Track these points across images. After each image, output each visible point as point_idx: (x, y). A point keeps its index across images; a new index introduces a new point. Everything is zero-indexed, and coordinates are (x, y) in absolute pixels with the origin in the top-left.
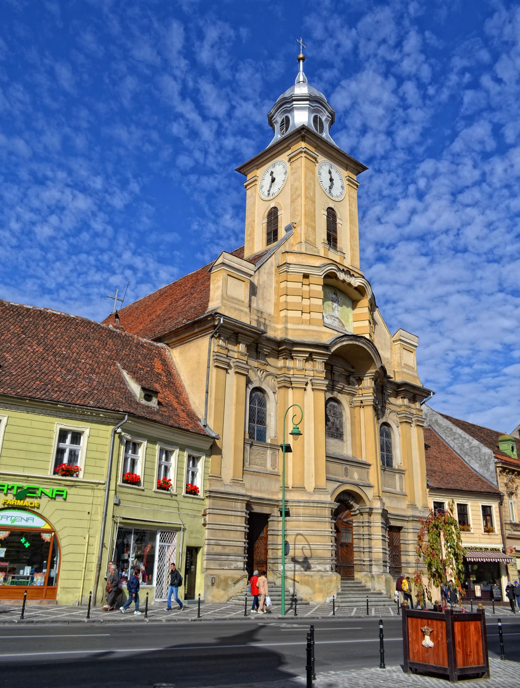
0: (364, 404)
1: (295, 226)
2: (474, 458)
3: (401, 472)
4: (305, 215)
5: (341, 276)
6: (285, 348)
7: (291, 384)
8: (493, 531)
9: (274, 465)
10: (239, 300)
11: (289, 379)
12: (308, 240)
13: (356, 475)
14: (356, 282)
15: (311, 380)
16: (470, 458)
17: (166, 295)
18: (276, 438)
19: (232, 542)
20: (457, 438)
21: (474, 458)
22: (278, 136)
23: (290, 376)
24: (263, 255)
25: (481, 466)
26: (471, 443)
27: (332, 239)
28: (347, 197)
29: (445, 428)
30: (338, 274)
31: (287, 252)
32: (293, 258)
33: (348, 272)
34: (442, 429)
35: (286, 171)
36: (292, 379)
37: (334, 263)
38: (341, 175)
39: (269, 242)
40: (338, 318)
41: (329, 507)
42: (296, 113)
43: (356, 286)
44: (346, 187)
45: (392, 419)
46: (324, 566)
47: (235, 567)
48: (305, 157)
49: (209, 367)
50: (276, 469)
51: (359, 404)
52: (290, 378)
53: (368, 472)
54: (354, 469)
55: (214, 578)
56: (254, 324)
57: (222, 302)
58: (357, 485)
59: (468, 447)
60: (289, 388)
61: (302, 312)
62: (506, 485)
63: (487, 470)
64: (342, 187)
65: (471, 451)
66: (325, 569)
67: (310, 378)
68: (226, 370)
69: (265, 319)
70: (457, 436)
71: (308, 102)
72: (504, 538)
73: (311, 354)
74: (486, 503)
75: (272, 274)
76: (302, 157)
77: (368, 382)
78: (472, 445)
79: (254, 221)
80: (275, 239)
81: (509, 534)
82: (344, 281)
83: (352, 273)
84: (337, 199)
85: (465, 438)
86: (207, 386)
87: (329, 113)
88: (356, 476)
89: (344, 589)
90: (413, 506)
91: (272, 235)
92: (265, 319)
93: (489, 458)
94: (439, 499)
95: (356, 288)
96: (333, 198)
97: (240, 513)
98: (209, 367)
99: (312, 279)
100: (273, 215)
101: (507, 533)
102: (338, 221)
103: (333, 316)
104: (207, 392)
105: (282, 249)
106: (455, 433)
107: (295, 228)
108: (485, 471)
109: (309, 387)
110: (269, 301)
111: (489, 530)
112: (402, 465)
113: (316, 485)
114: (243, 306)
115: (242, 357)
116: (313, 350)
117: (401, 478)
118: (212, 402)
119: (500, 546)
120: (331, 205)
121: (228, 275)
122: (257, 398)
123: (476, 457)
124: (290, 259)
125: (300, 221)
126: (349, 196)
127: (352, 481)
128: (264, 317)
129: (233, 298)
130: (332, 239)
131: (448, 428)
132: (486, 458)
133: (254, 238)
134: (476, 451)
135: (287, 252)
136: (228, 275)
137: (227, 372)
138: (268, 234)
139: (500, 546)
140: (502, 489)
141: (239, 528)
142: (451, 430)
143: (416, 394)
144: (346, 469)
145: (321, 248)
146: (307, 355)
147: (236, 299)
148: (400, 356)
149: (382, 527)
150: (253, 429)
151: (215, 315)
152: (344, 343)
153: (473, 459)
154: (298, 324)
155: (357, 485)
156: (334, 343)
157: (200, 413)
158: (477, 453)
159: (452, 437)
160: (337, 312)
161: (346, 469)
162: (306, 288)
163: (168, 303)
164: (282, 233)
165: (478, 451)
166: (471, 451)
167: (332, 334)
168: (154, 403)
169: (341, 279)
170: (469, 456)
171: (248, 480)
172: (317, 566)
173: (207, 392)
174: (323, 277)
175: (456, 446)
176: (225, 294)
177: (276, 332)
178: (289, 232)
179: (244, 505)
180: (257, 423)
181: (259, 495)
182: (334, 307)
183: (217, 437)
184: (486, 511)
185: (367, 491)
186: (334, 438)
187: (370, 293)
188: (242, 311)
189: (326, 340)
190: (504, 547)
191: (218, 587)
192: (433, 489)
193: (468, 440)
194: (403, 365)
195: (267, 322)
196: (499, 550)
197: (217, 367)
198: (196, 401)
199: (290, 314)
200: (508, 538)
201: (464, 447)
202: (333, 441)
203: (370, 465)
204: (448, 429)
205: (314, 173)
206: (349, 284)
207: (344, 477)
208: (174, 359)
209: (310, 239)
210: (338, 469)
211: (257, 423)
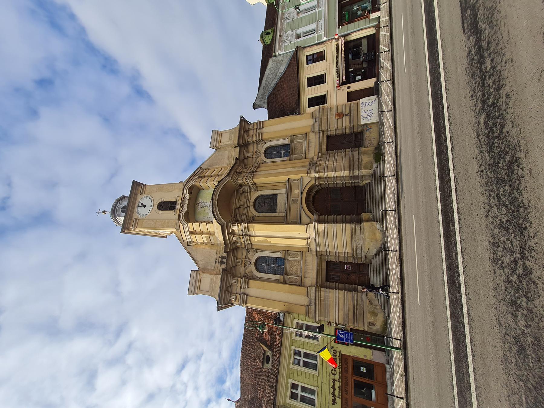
13: (296, 192)
25: (281, 65)
53: (294, 180)
60: (252, 244)
109: (249, 233)
127: (300, 195)
175: (273, 82)
179: (322, 289)
185: (305, 183)
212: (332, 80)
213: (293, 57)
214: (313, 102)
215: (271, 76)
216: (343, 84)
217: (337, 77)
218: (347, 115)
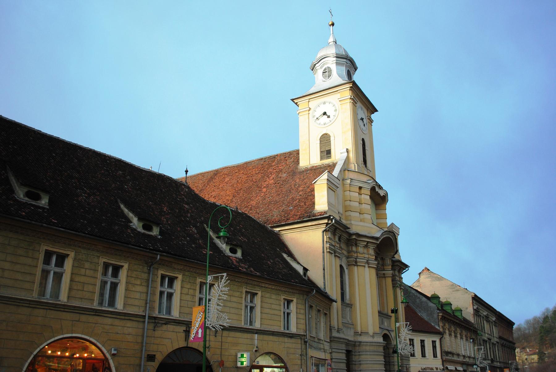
8: (436, 357)
58: (388, 330)
71: (345, 60)
72: (443, 361)
73: (368, 242)
98: (324, 252)
99: (363, 191)
101: (444, 358)
104: (324, 269)
111: (435, 356)
138: (321, 152)
173: (324, 269)
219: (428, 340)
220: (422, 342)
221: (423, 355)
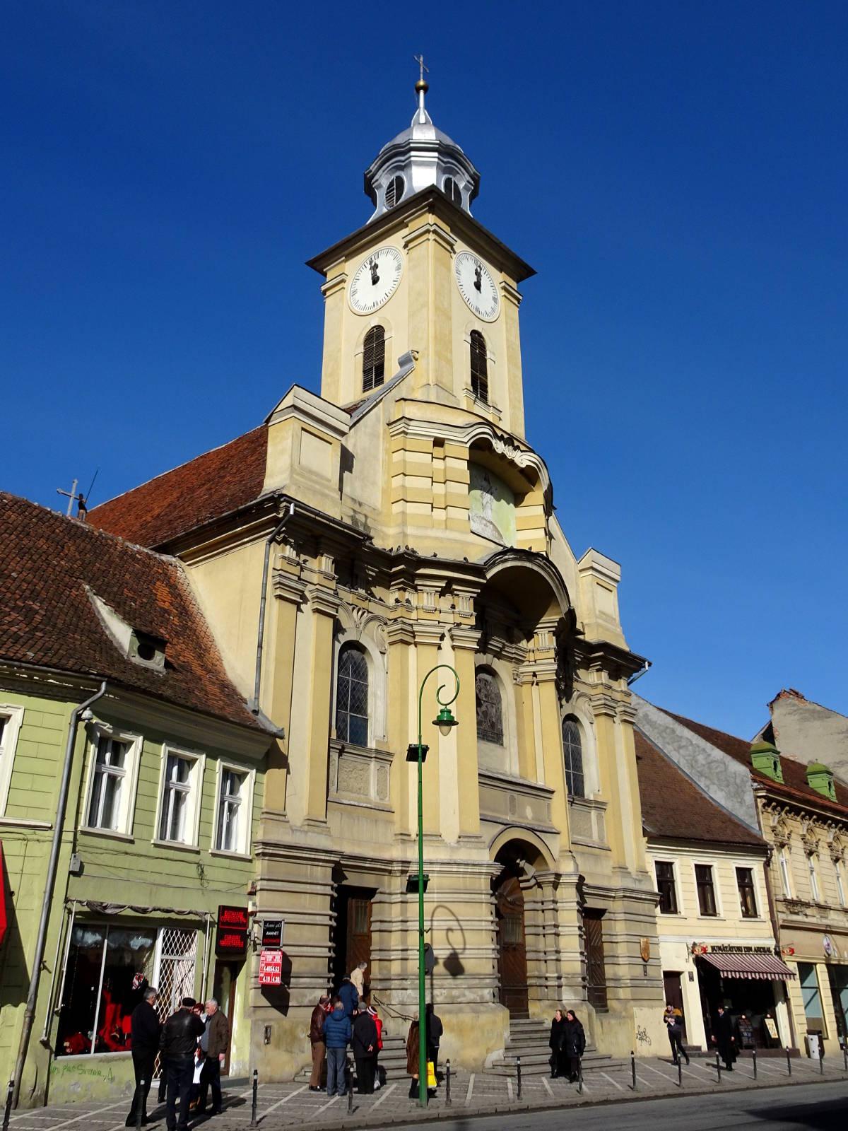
0: (540, 678)
1: (417, 356)
2: (716, 782)
3: (600, 806)
4: (436, 338)
5: (499, 447)
6: (405, 568)
7: (414, 637)
8: (755, 915)
9: (382, 792)
10: (322, 477)
11: (409, 628)
12: (441, 383)
13: (528, 811)
14: (523, 459)
15: (450, 630)
16: (708, 782)
17: (170, 484)
18: (386, 739)
19: (305, 949)
20: (684, 746)
21: (716, 782)
22: (382, 208)
23: (411, 622)
24: (357, 408)
25: (729, 796)
26: (709, 755)
27: (479, 385)
28: (503, 318)
29: (661, 728)
30: (494, 441)
31: (405, 400)
32: (415, 411)
33: (509, 440)
34: (656, 731)
35: (400, 265)
36: (416, 628)
37: (488, 423)
38: (494, 278)
39: (367, 386)
40: (491, 523)
41: (487, 874)
42: (415, 170)
43: (523, 466)
44: (501, 300)
45: (582, 708)
46: (480, 992)
47: (310, 1001)
48: (435, 240)
49: (264, 598)
50: (387, 799)
51: (530, 678)
52: (411, 625)
53: (549, 805)
54: (526, 799)
55: (270, 1027)
56: (348, 521)
57: (291, 477)
58: (532, 830)
59: (704, 762)
60: (408, 644)
61: (433, 507)
62: (774, 829)
63: (741, 802)
64: (495, 299)
65: (710, 768)
66: (482, 997)
67: (448, 627)
68: (298, 605)
69: (366, 516)
70: (684, 743)
73: (451, 581)
74: (744, 863)
75: (378, 437)
76: (428, 239)
77: (544, 641)
78: (711, 758)
79: (340, 350)
80: (380, 380)
81: (784, 921)
82: (503, 456)
83: (516, 443)
84: (486, 319)
85: (698, 747)
86: (261, 634)
87: (471, 177)
88: (529, 813)
89: (516, 1037)
90: (622, 869)
91: (374, 372)
92: (366, 516)
93: (742, 781)
94: (665, 857)
95: (522, 471)
96: (480, 316)
97: (322, 887)
98: (264, 598)
100: (375, 341)
101: (781, 918)
102: (489, 355)
103: (483, 518)
104: (260, 646)
105: (396, 394)
106: (681, 737)
107: (417, 360)
108: (737, 805)
109: (447, 643)
110: (374, 483)
111: (749, 911)
112: (600, 793)
113: (461, 830)
114: (327, 487)
115: (326, 583)
116: (455, 574)
117: (600, 818)
118: (269, 666)
119: (771, 943)
120: (478, 327)
121: (303, 429)
122: (350, 663)
123: (719, 779)
124: (410, 410)
125: (427, 348)
126: (506, 316)
127: (524, 823)
128: (365, 512)
129: (311, 472)
130: (479, 385)
131: (667, 727)
132: (738, 781)
133: (338, 381)
134: (719, 770)
135: (405, 400)
136: (303, 429)
137: (299, 609)
138: (366, 372)
139: (771, 943)
140: (768, 837)
141: (318, 919)
142: (673, 731)
143: (621, 664)
144: (512, 799)
145: (464, 398)
146: (443, 584)
147: (317, 474)
148: (593, 596)
149: (578, 911)
150: (345, 721)
151: (277, 499)
152: (509, 564)
153: (714, 784)
154: (426, 528)
155: (532, 830)
156: (491, 563)
157: (247, 691)
158: (721, 772)
159: (676, 744)
160: (490, 511)
161: (512, 799)
162: (438, 464)
163: (175, 495)
164: (392, 369)
165: (723, 769)
166: (710, 768)
167: (486, 547)
168: (157, 662)
169: (499, 451)
170: (706, 777)
171: (334, 821)
172: (467, 992)
173: (260, 646)
174: (468, 445)
176: (294, 463)
177: (386, 539)
178: (407, 367)
179: (329, 871)
180: (350, 711)
181: (357, 851)
182: (484, 503)
183: (280, 734)
184: (744, 876)
186: (488, 740)
187: (547, 482)
188: (326, 496)
189: (477, 558)
190: (777, 945)
191: (277, 1046)
192: (656, 837)
193: (704, 750)
194: (597, 612)
195: (369, 522)
196: (769, 950)
197: (280, 597)
198: (237, 664)
199: (410, 508)
200: (783, 927)
201: (696, 761)
202: (490, 747)
203: (553, 792)
204: (668, 731)
205: (449, 270)
206: (512, 462)
207: (510, 815)
208: (193, 586)
209: (444, 381)
210: (500, 797)
211: (350, 711)
212: (711, 934)
213: (746, 830)
214: (665, 870)
215: (701, 758)
216: (699, 962)
217: (713, 948)
218: (645, 972)
219: (724, 869)
220: (704, 874)
221: (708, 907)
